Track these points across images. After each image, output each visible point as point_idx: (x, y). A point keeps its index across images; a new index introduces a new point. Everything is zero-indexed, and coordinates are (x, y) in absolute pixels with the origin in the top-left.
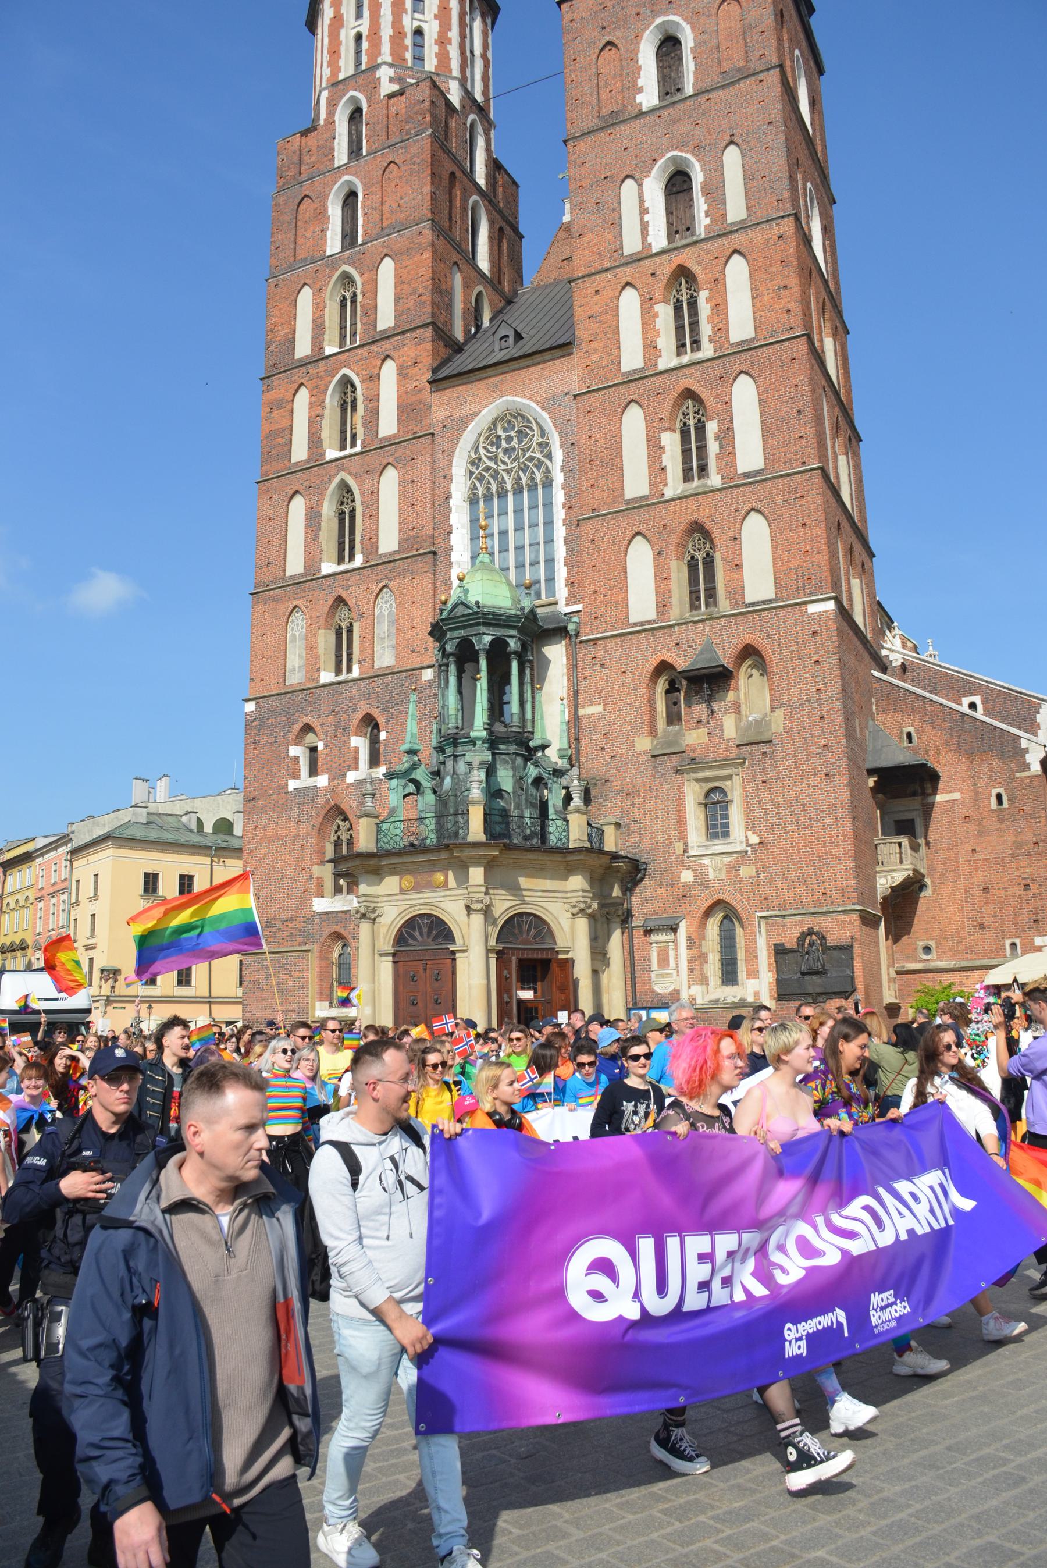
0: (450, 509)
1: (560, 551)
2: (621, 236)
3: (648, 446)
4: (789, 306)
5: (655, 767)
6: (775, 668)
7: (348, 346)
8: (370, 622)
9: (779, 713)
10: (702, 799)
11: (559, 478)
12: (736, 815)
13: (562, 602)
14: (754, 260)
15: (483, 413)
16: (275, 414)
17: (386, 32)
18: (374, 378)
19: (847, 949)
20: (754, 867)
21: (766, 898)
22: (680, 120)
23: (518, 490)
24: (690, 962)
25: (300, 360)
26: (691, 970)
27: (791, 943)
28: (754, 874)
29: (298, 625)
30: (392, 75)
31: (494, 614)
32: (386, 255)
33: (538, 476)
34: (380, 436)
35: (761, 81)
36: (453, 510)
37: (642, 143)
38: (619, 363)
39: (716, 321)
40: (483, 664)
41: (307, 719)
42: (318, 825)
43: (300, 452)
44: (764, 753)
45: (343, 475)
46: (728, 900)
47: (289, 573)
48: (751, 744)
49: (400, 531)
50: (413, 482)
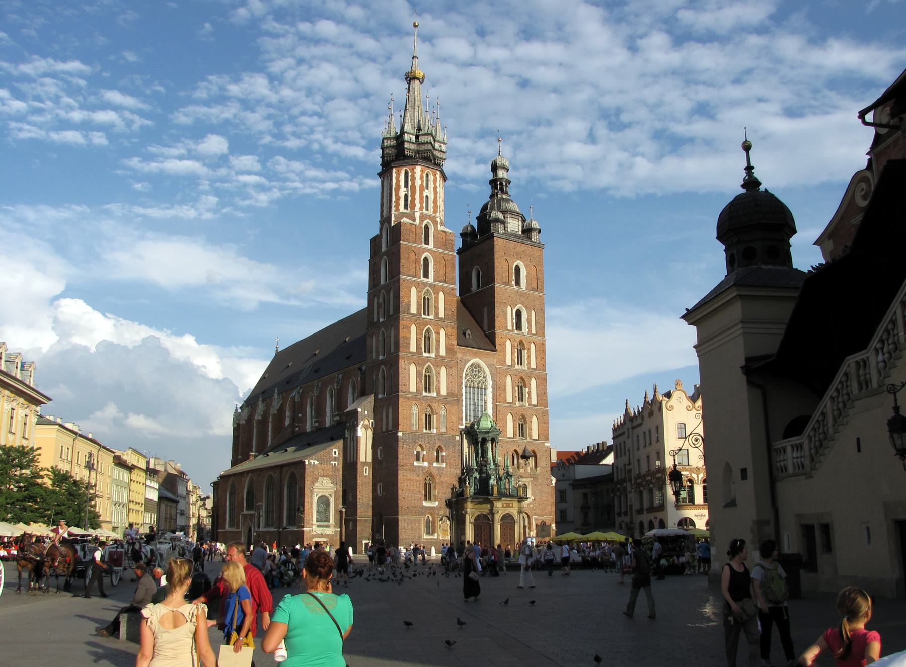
4: (544, 364)
6: (538, 457)
7: (427, 317)
16: (404, 330)
18: (438, 333)
23: (478, 388)
25: (413, 314)
27: (539, 524)
33: (484, 387)
34: (440, 354)
35: (540, 296)
41: (420, 443)
45: (429, 363)
47: (411, 391)
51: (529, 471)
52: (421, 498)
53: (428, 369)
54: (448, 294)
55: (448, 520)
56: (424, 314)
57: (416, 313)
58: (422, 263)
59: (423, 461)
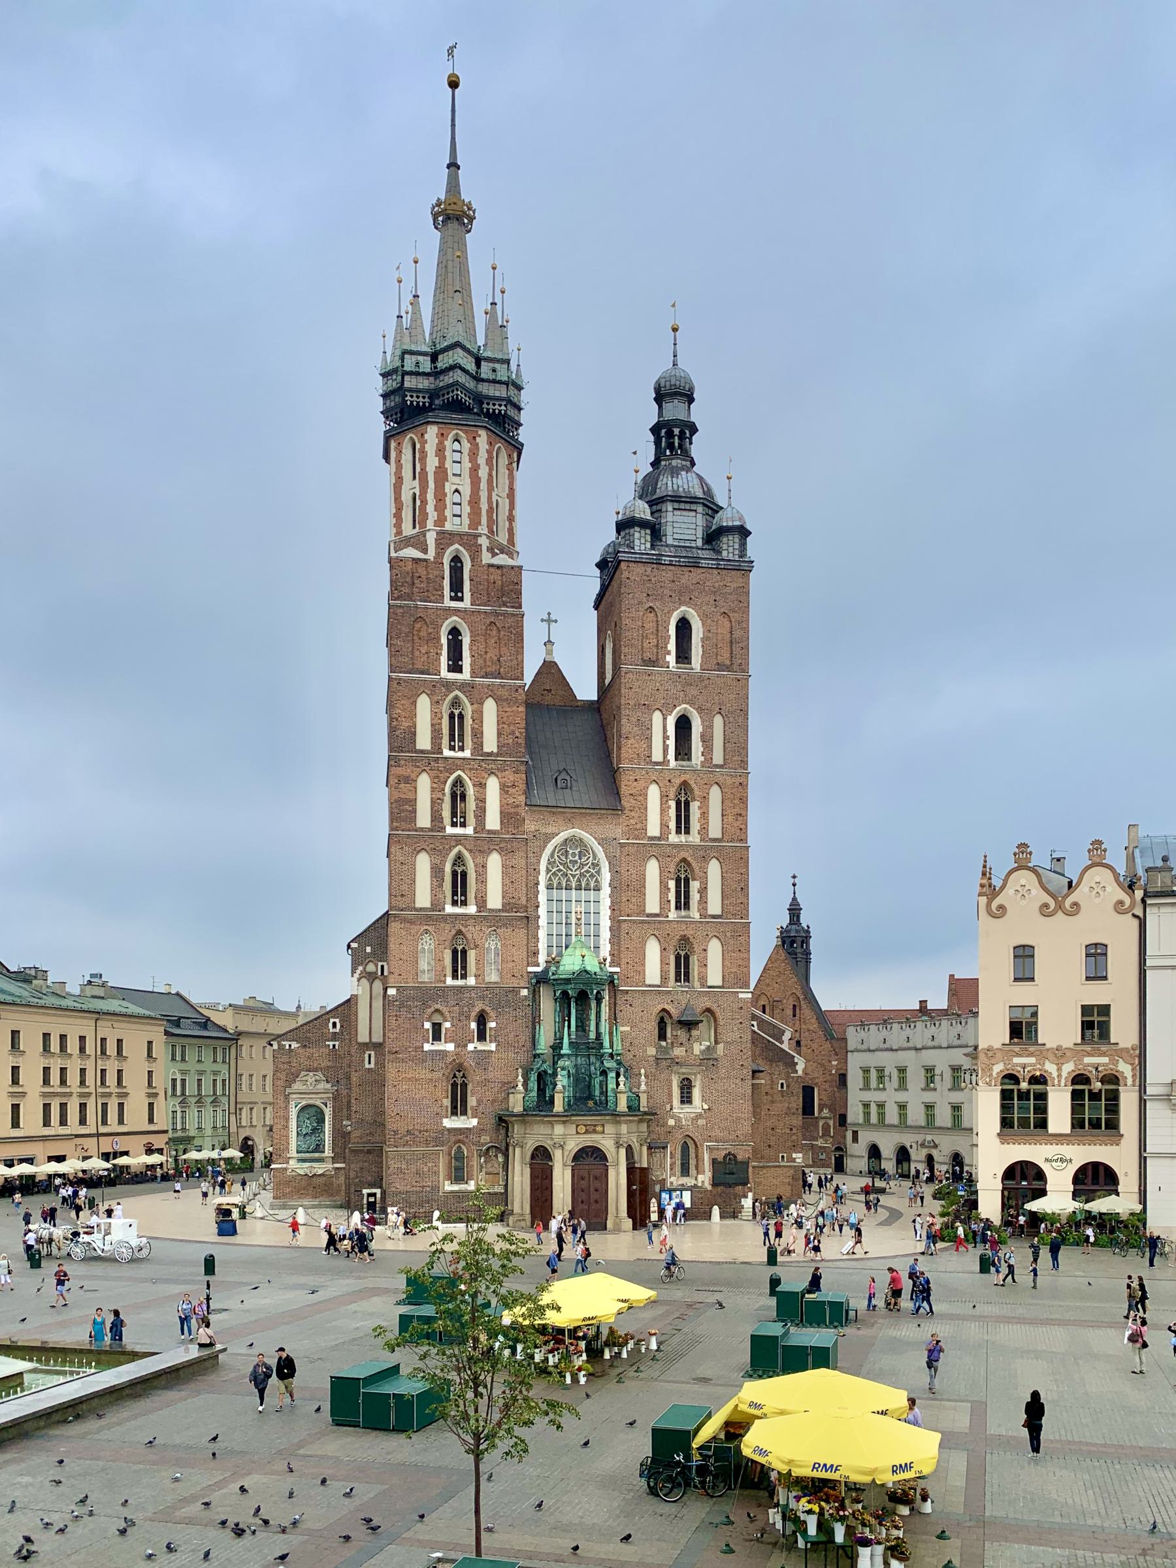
1: (605, 934)
5: (657, 1064)
7: (460, 754)
9: (720, 1046)
11: (606, 890)
12: (696, 1093)
16: (402, 786)
18: (481, 786)
19: (746, 1164)
26: (671, 1169)
27: (720, 1159)
33: (592, 885)
34: (488, 827)
41: (438, 1006)
42: (446, 1074)
43: (424, 820)
47: (418, 905)
49: (503, 897)
51: (697, 1051)
53: (459, 859)
54: (507, 699)
55: (499, 1155)
56: (452, 748)
57: (429, 748)
58: (444, 641)
59: (446, 1042)
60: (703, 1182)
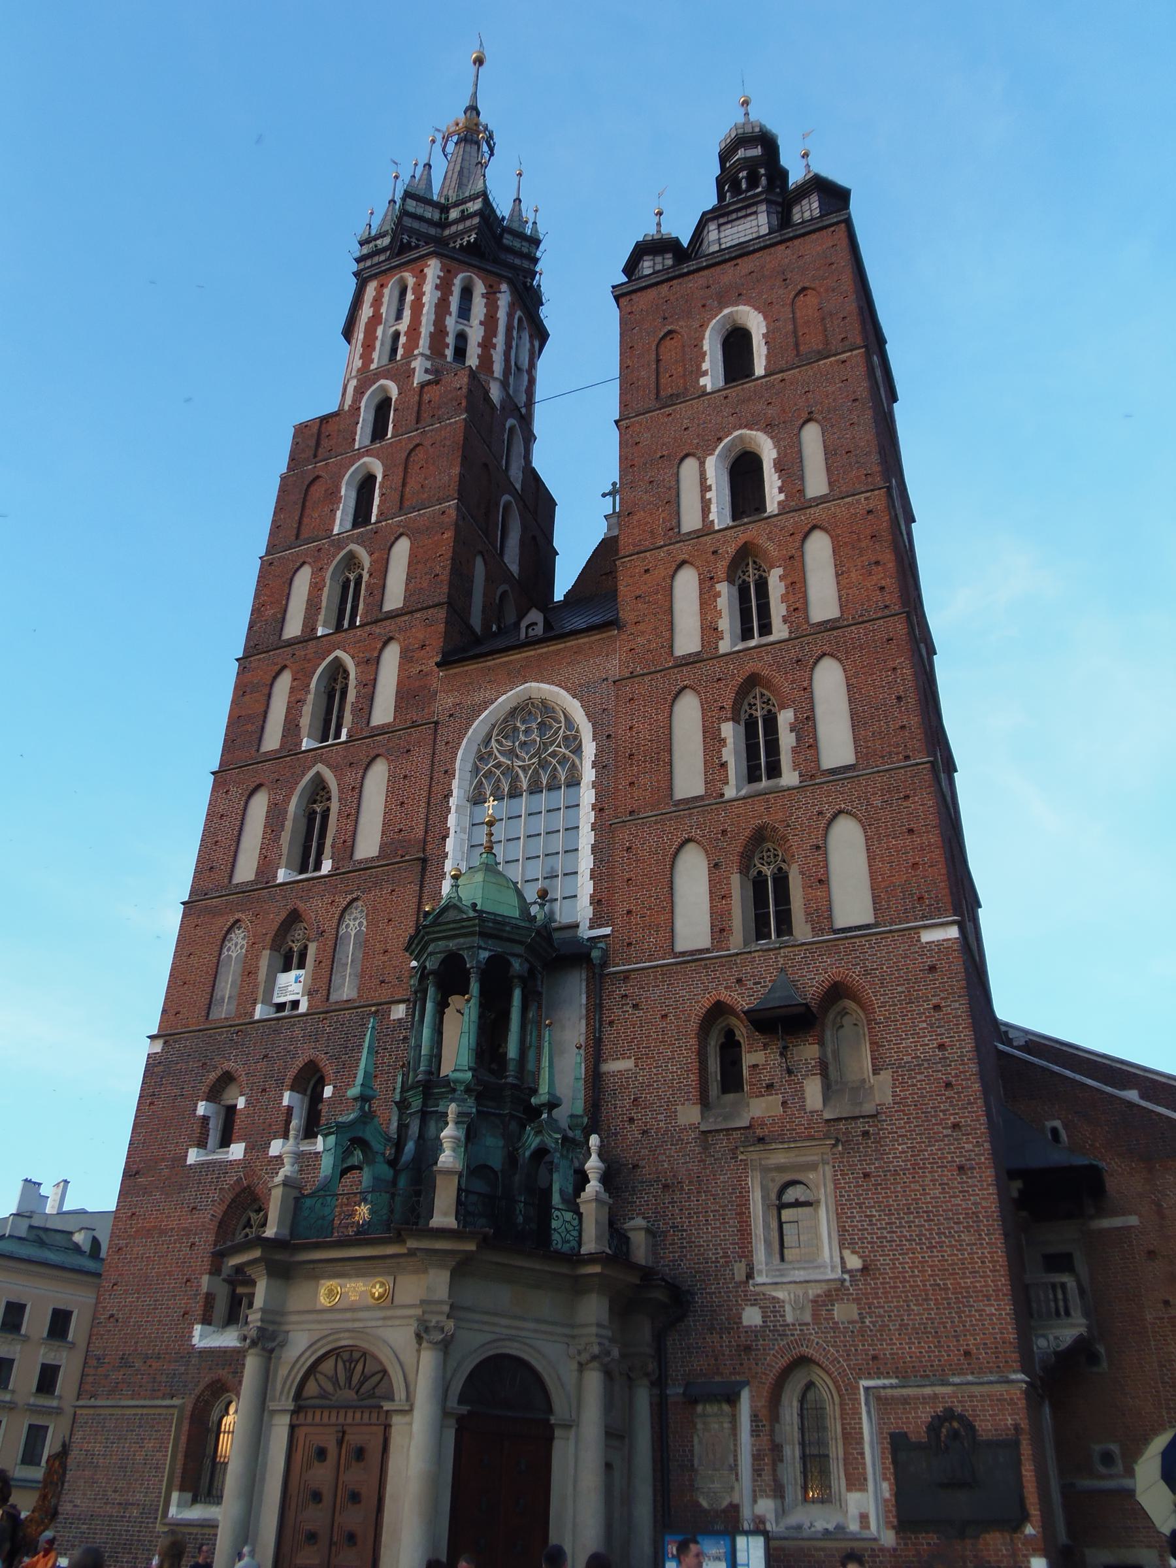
0: (449, 810)
1: (585, 862)
2: (678, 514)
3: (705, 737)
4: (883, 583)
5: (705, 1148)
8: (331, 943)
9: (886, 1076)
10: (773, 1196)
11: (588, 774)
13: (585, 924)
14: (839, 535)
15: (500, 700)
16: (247, 697)
17: (426, 327)
18: (371, 663)
20: (855, 1306)
21: (875, 1358)
22: (749, 399)
24: (757, 1457)
26: (757, 1472)
28: (856, 1317)
29: (236, 946)
30: (429, 367)
31: (495, 922)
32: (401, 535)
33: (562, 776)
35: (844, 362)
36: (453, 810)
37: (704, 423)
38: (671, 647)
39: (793, 600)
40: (474, 987)
41: (230, 1066)
43: (272, 740)
44: (866, 1134)
45: (320, 767)
46: (816, 1356)
47: (236, 880)
48: (846, 1119)
50: (405, 777)
52: (185, 1313)
53: (319, 789)
56: (339, 628)
60: (864, 1518)
